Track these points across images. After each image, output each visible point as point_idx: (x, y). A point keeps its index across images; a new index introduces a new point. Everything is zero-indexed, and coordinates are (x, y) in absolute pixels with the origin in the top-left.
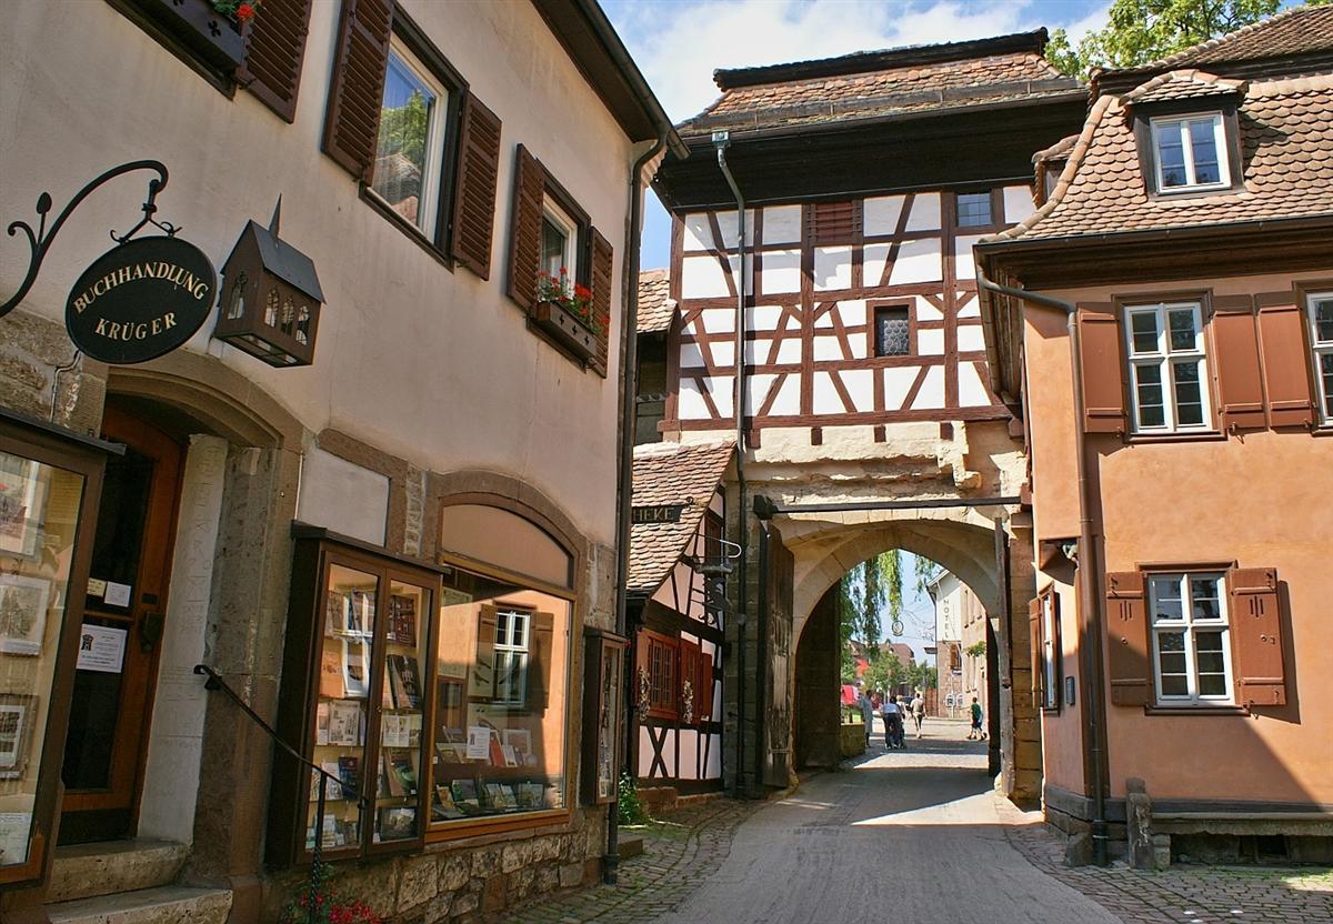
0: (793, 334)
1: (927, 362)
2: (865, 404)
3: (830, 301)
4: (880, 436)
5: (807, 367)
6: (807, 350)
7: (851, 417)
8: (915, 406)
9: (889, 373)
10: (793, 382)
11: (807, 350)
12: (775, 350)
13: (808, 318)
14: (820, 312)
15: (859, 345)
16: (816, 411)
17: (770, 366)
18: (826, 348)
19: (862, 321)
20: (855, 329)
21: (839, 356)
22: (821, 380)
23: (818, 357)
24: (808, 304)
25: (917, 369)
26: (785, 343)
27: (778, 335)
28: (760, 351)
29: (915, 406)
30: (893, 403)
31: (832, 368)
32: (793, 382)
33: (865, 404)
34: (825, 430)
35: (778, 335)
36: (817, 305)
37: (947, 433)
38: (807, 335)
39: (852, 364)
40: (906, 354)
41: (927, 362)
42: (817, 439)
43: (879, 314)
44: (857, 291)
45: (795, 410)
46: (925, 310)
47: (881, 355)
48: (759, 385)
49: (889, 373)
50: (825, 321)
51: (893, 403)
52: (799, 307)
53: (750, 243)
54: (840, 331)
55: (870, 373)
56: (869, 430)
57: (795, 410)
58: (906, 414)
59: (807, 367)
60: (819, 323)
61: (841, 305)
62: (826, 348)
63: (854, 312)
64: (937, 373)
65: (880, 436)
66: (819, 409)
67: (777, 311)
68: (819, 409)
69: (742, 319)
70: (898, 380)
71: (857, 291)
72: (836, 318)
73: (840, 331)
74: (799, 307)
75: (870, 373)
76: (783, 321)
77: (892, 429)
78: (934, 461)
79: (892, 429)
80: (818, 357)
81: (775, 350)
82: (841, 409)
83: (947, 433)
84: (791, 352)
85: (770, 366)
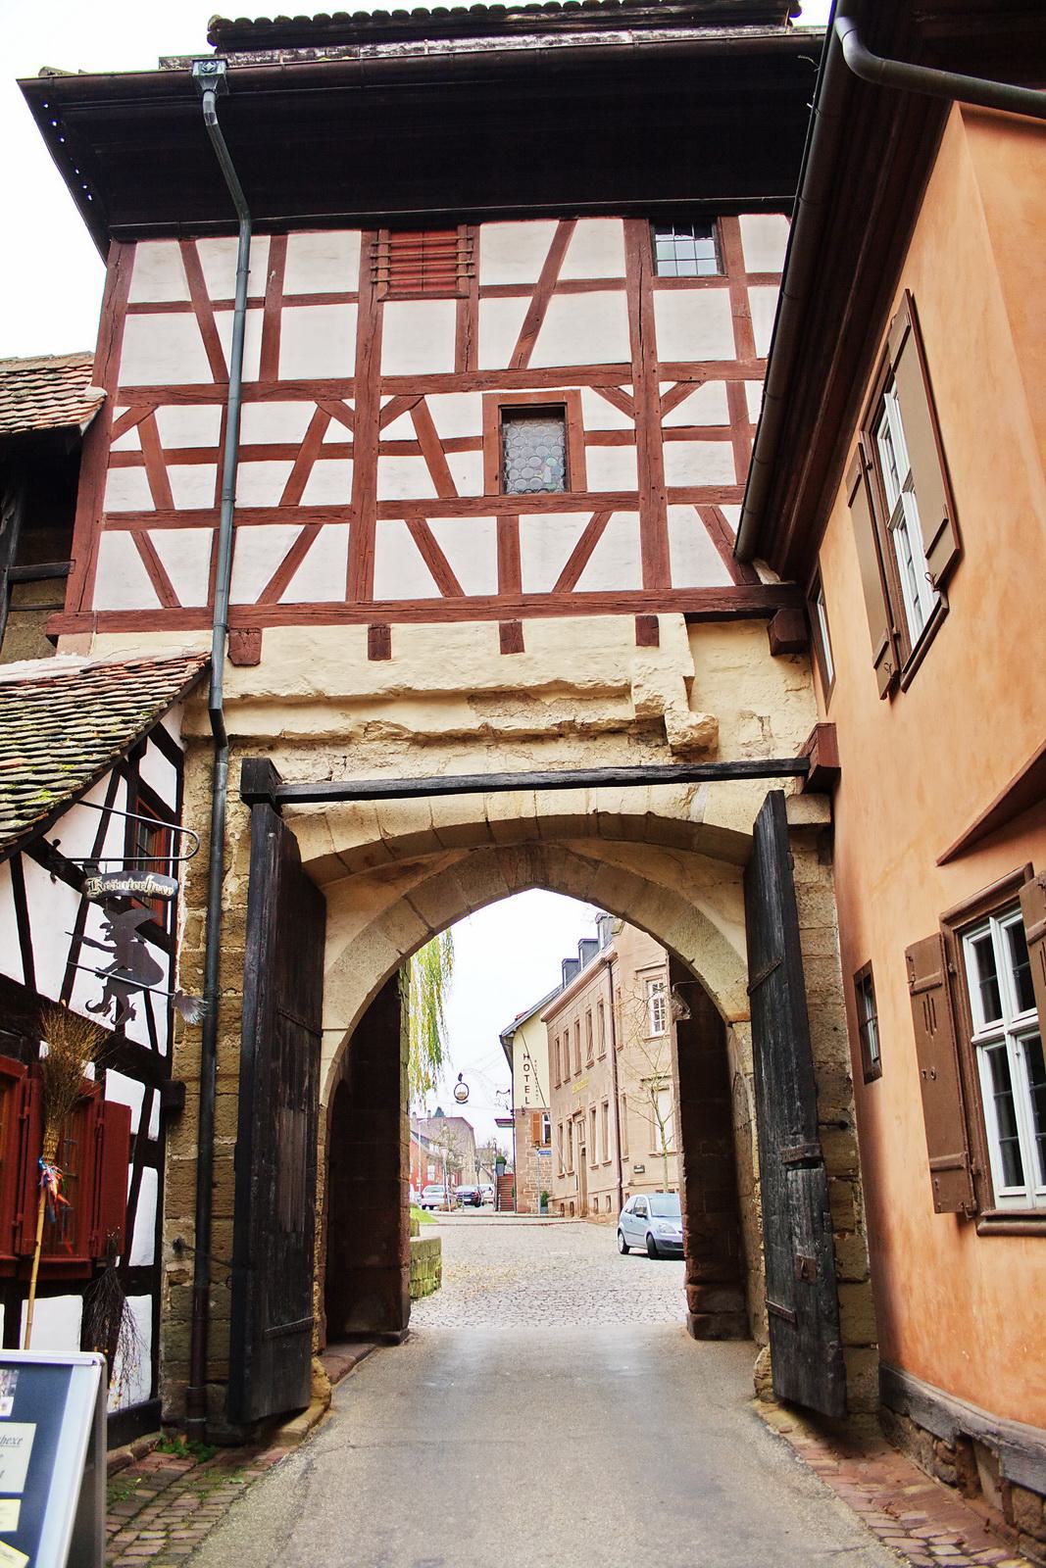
0: (337, 451)
2: (479, 579)
4: (512, 641)
8: (585, 584)
12: (297, 482)
13: (367, 423)
14: (392, 412)
15: (469, 473)
17: (288, 510)
22: (392, 538)
23: (385, 492)
26: (320, 467)
27: (303, 455)
30: (538, 577)
32: (334, 538)
33: (479, 579)
34: (399, 632)
35: (303, 455)
37: (648, 634)
38: (365, 454)
39: (452, 505)
45: (336, 592)
51: (538, 577)
54: (431, 448)
58: (564, 601)
65: (512, 641)
73: (431, 448)
76: (318, 427)
77: (533, 629)
79: (533, 629)
80: (385, 492)
81: (297, 482)
83: (648, 634)
84: (331, 483)
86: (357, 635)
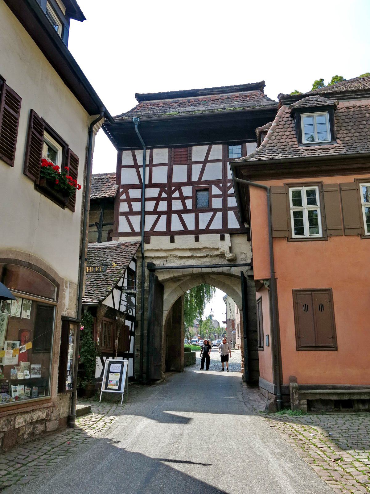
0: (163, 199)
1: (216, 211)
2: (191, 226)
3: (179, 186)
4: (197, 239)
5: (169, 212)
6: (169, 205)
7: (186, 232)
8: (211, 228)
9: (201, 215)
10: (164, 218)
11: (169, 205)
12: (157, 206)
13: (170, 193)
14: (175, 190)
15: (189, 204)
17: (155, 212)
18: (177, 205)
19: (190, 194)
20: (188, 198)
21: (181, 207)
22: (175, 217)
23: (174, 208)
24: (170, 188)
25: (211, 214)
26: (161, 203)
27: (158, 200)
28: (150, 206)
29: (211, 228)
30: (202, 226)
31: (179, 212)
32: (164, 218)
33: (191, 226)
34: (176, 237)
35: (158, 200)
36: (173, 188)
38: (169, 200)
39: (186, 211)
40: (209, 208)
41: (216, 211)
42: (172, 241)
43: (196, 191)
44: (189, 183)
45: (164, 229)
46: (215, 191)
47: (196, 210)
48: (150, 220)
49: (201, 215)
50: (176, 194)
51: (202, 226)
52: (167, 189)
53: (148, 163)
54: (182, 198)
55: (193, 215)
56: (192, 237)
57: (164, 229)
58: (207, 231)
59: (169, 212)
61: (182, 188)
62: (177, 205)
63: (187, 191)
64: (219, 215)
65: (197, 239)
66: (173, 229)
67: (157, 190)
68: (173, 229)
69: (143, 193)
70: (204, 218)
71: (189, 183)
72: (181, 193)
73: (182, 198)
74: (167, 189)
75: (193, 215)
76: (160, 194)
77: (201, 237)
78: (218, 249)
79: (201, 237)
80: (174, 208)
82: (182, 229)
83: (222, 238)
84: (163, 206)
85: (155, 212)
86: (168, 238)
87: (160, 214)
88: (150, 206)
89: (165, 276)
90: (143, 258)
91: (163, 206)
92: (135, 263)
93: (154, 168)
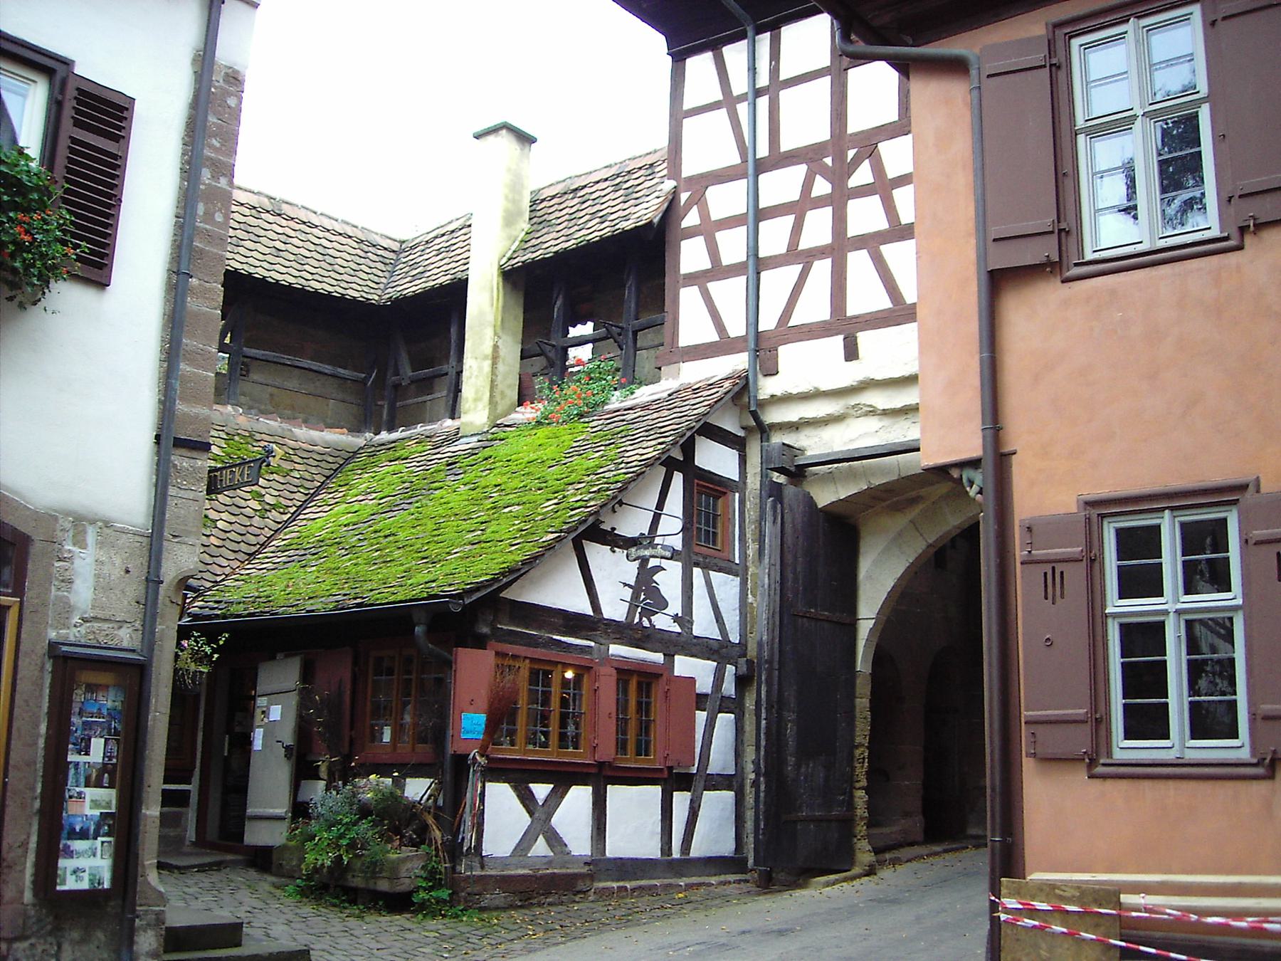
0: (820, 202)
3: (869, 144)
5: (839, 248)
13: (839, 175)
14: (857, 162)
16: (851, 312)
20: (903, 180)
21: (879, 222)
22: (858, 261)
23: (853, 230)
24: (840, 156)
27: (799, 209)
28: (774, 236)
31: (871, 242)
32: (822, 269)
35: (799, 209)
36: (851, 153)
38: (839, 201)
39: (900, 232)
48: (776, 284)
50: (863, 176)
52: (828, 161)
59: (839, 248)
60: (856, 180)
61: (884, 148)
66: (855, 307)
68: (855, 307)
72: (878, 169)
73: (883, 187)
76: (808, 184)
80: (853, 230)
87: (806, 258)
88: (774, 236)
89: (840, 489)
90: (764, 430)
91: (818, 228)
92: (735, 453)
93: (719, 96)
